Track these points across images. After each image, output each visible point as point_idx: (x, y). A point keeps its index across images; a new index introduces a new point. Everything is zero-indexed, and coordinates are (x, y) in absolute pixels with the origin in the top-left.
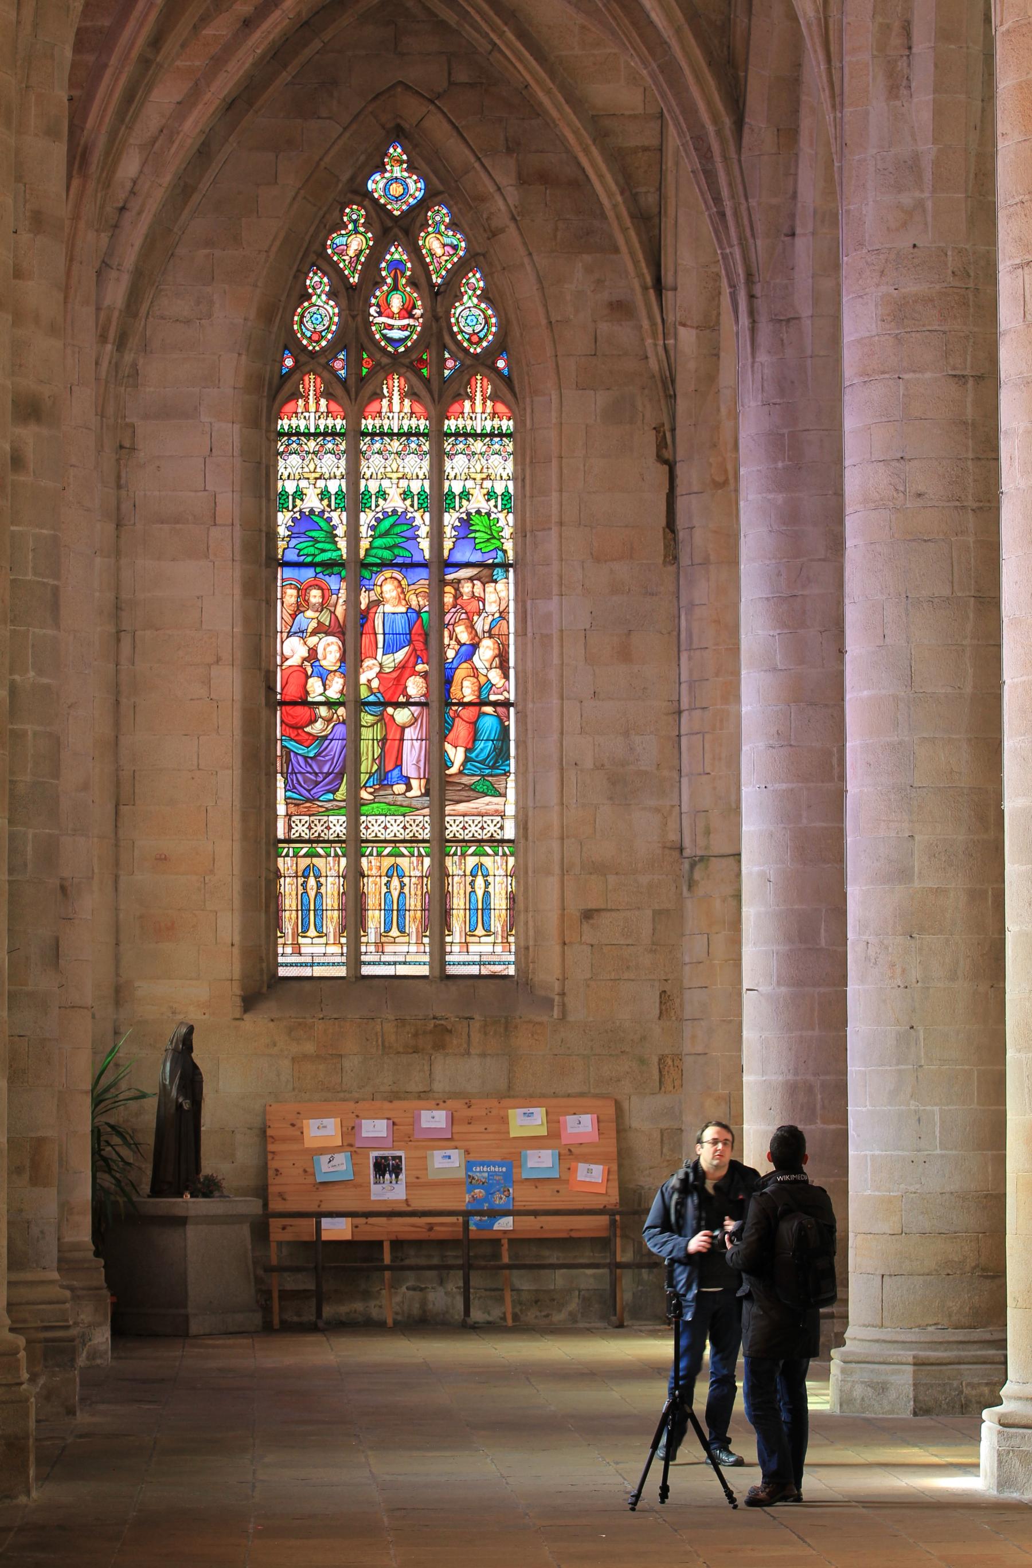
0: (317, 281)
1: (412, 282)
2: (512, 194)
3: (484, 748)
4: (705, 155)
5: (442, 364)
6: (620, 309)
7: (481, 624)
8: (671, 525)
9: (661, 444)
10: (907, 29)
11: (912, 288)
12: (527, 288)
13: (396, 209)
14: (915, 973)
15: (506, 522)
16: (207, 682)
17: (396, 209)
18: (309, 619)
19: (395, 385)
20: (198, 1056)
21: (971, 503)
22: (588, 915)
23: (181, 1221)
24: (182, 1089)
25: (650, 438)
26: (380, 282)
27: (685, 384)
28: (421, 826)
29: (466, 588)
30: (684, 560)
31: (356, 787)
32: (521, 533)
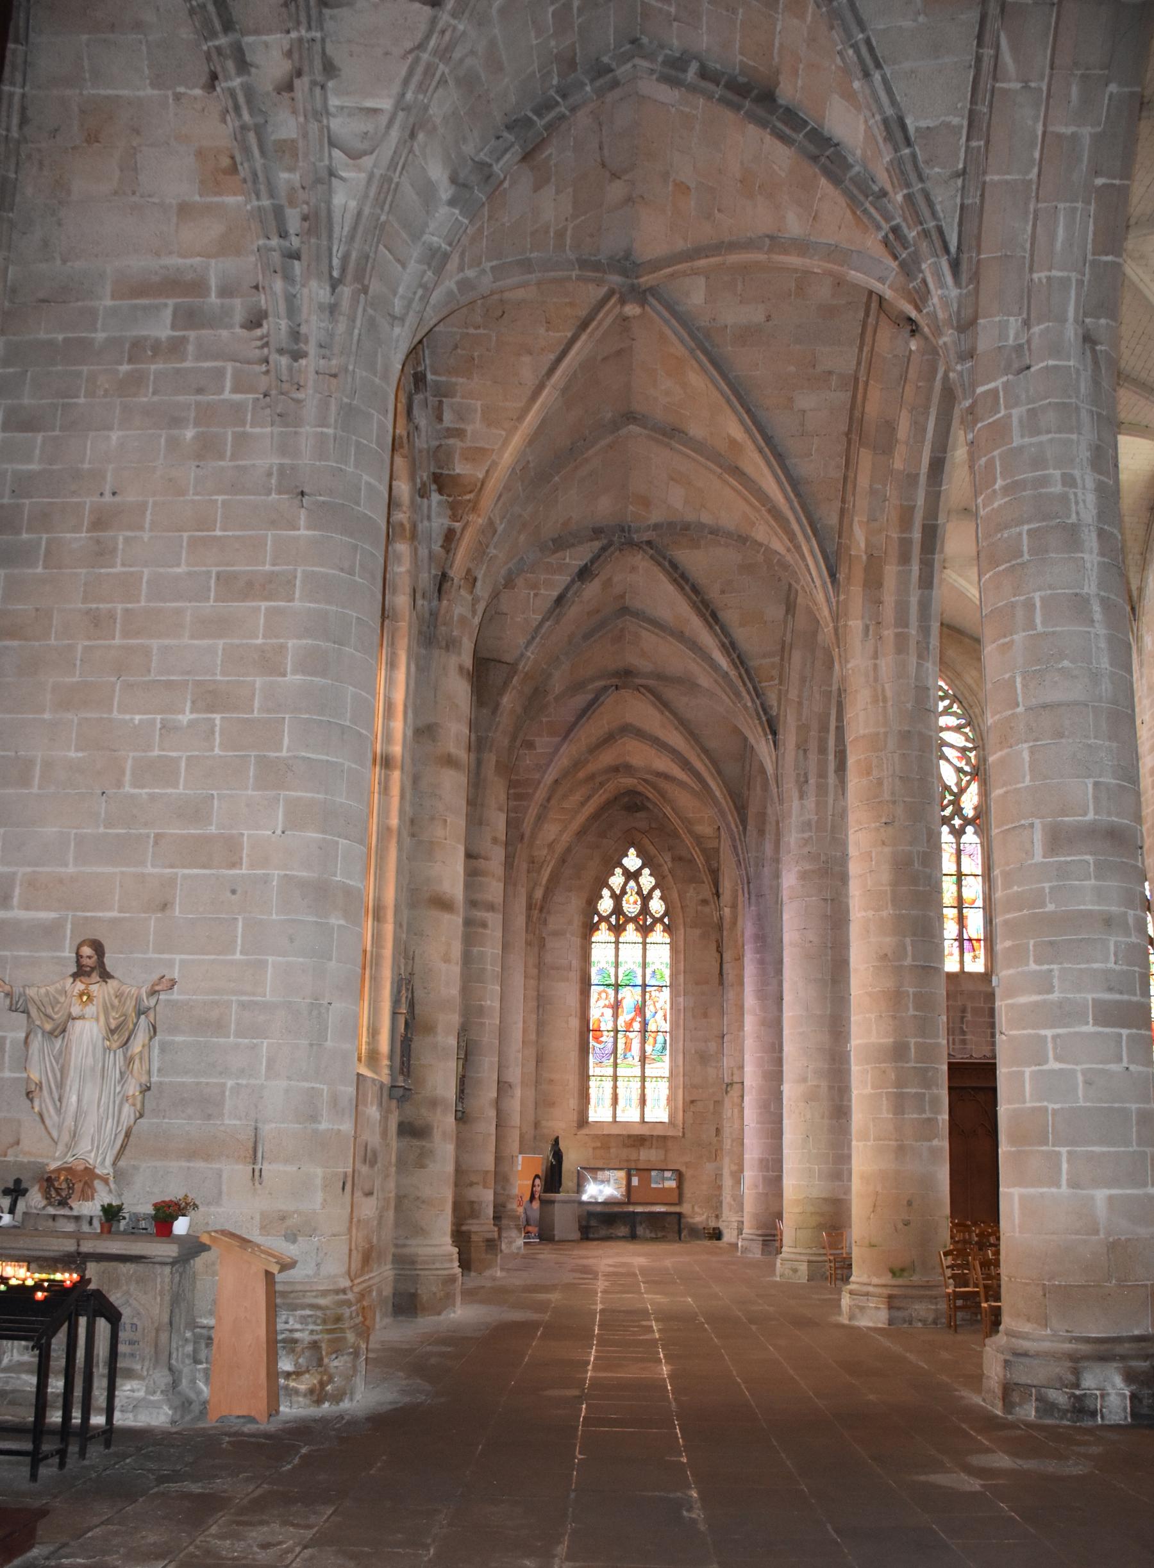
0: (606, 893)
1: (637, 893)
2: (670, 864)
3: (659, 1046)
4: (733, 840)
5: (646, 920)
6: (705, 902)
7: (658, 1005)
8: (721, 973)
9: (718, 947)
10: (806, 775)
11: (808, 867)
12: (675, 895)
13: (632, 869)
14: (809, 1116)
15: (667, 972)
16: (567, 1022)
17: (632, 869)
18: (602, 1003)
19: (631, 927)
20: (562, 1145)
21: (829, 945)
22: (692, 1102)
23: (553, 1202)
24: (554, 1157)
25: (714, 946)
26: (626, 893)
27: (726, 925)
28: (637, 1071)
29: (653, 994)
30: (726, 984)
31: (616, 1058)
32: (672, 976)
